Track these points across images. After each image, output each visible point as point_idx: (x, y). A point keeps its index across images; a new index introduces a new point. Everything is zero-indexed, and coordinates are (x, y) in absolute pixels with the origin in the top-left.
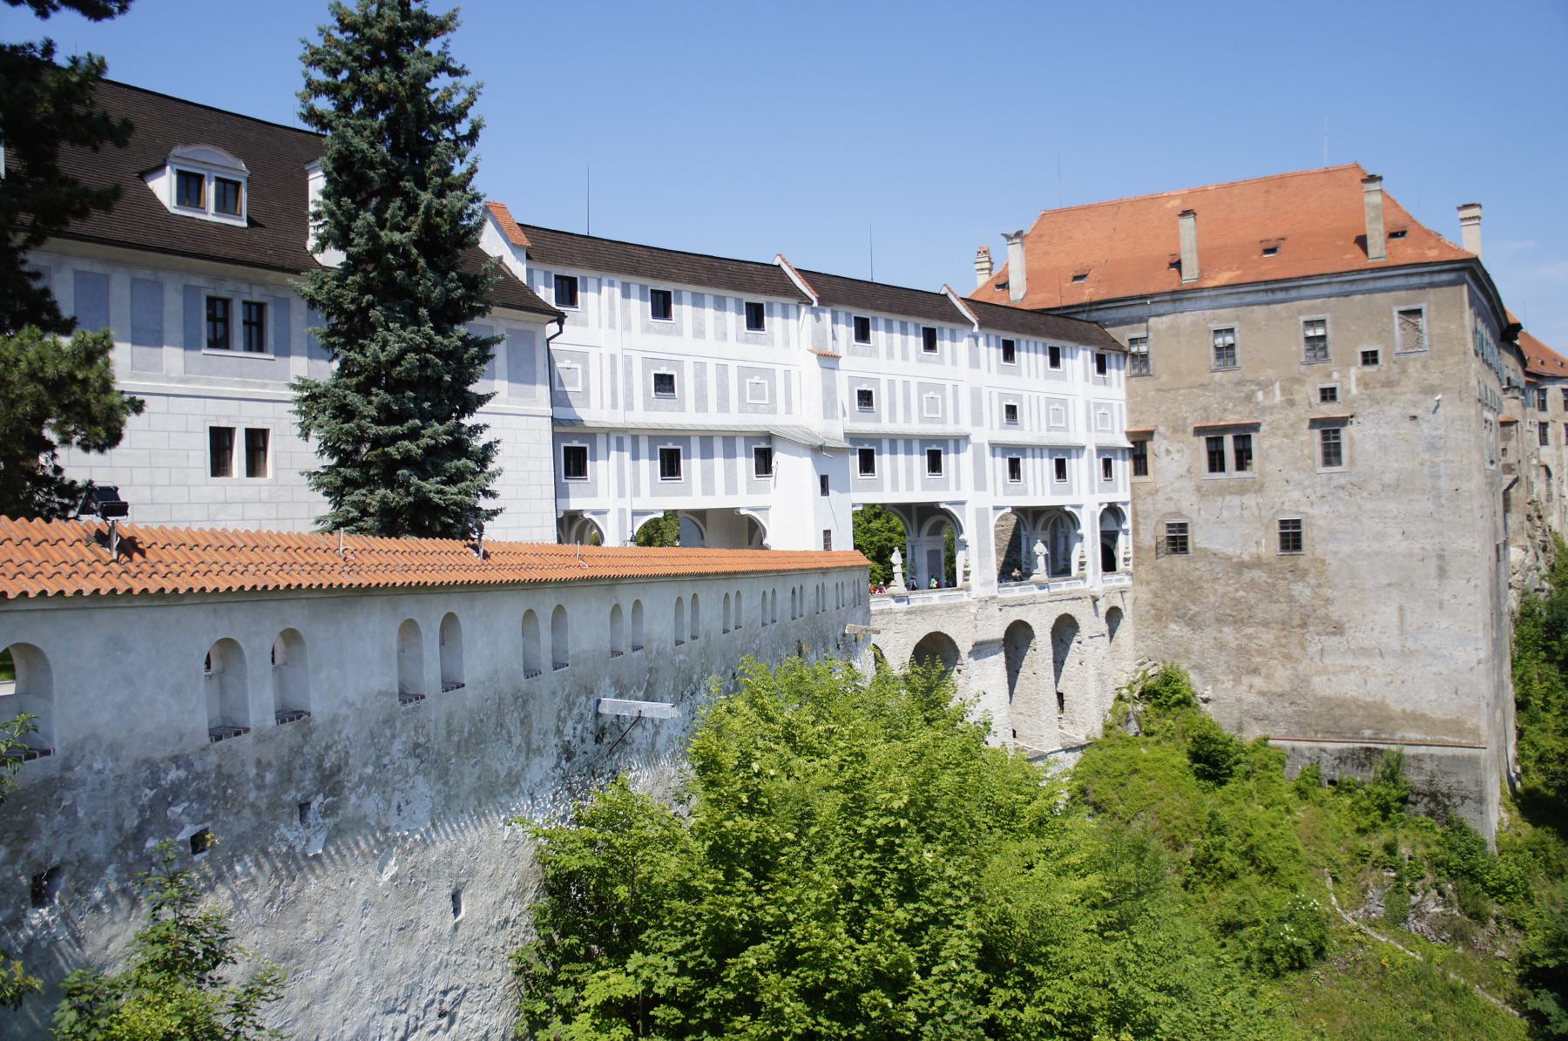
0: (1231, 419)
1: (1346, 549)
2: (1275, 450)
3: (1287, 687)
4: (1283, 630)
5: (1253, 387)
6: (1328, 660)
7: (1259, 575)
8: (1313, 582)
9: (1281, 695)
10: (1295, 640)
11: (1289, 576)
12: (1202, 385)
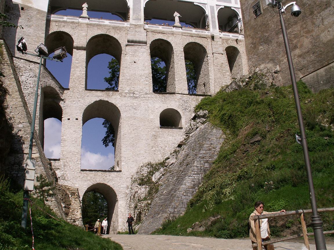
3: (310, 46)
4: (303, 21)
6: (326, 23)
9: (308, 52)
10: (309, 23)
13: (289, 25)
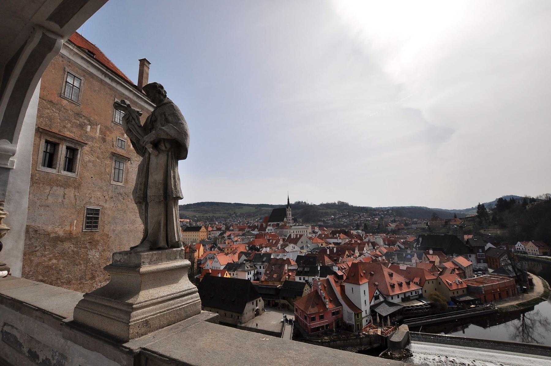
0: (68, 134)
1: (119, 228)
2: (91, 164)
4: (80, 284)
5: (86, 121)
7: (69, 246)
8: (101, 248)
11: (88, 245)
12: (51, 102)
13: (58, 280)
